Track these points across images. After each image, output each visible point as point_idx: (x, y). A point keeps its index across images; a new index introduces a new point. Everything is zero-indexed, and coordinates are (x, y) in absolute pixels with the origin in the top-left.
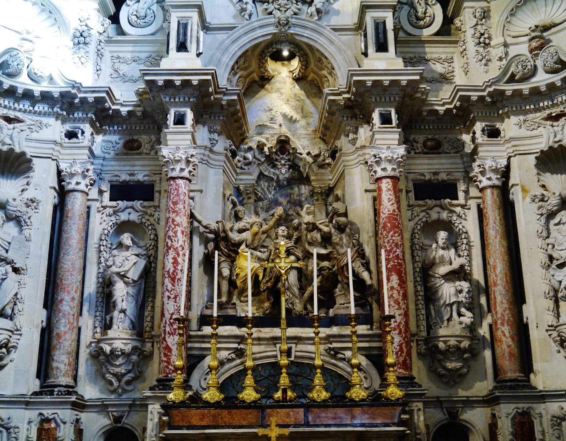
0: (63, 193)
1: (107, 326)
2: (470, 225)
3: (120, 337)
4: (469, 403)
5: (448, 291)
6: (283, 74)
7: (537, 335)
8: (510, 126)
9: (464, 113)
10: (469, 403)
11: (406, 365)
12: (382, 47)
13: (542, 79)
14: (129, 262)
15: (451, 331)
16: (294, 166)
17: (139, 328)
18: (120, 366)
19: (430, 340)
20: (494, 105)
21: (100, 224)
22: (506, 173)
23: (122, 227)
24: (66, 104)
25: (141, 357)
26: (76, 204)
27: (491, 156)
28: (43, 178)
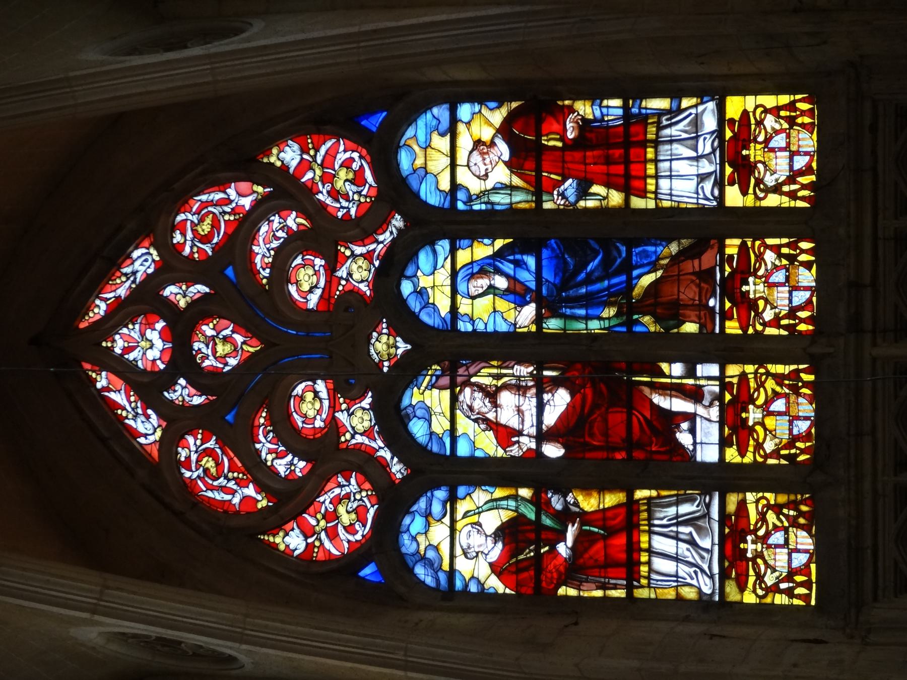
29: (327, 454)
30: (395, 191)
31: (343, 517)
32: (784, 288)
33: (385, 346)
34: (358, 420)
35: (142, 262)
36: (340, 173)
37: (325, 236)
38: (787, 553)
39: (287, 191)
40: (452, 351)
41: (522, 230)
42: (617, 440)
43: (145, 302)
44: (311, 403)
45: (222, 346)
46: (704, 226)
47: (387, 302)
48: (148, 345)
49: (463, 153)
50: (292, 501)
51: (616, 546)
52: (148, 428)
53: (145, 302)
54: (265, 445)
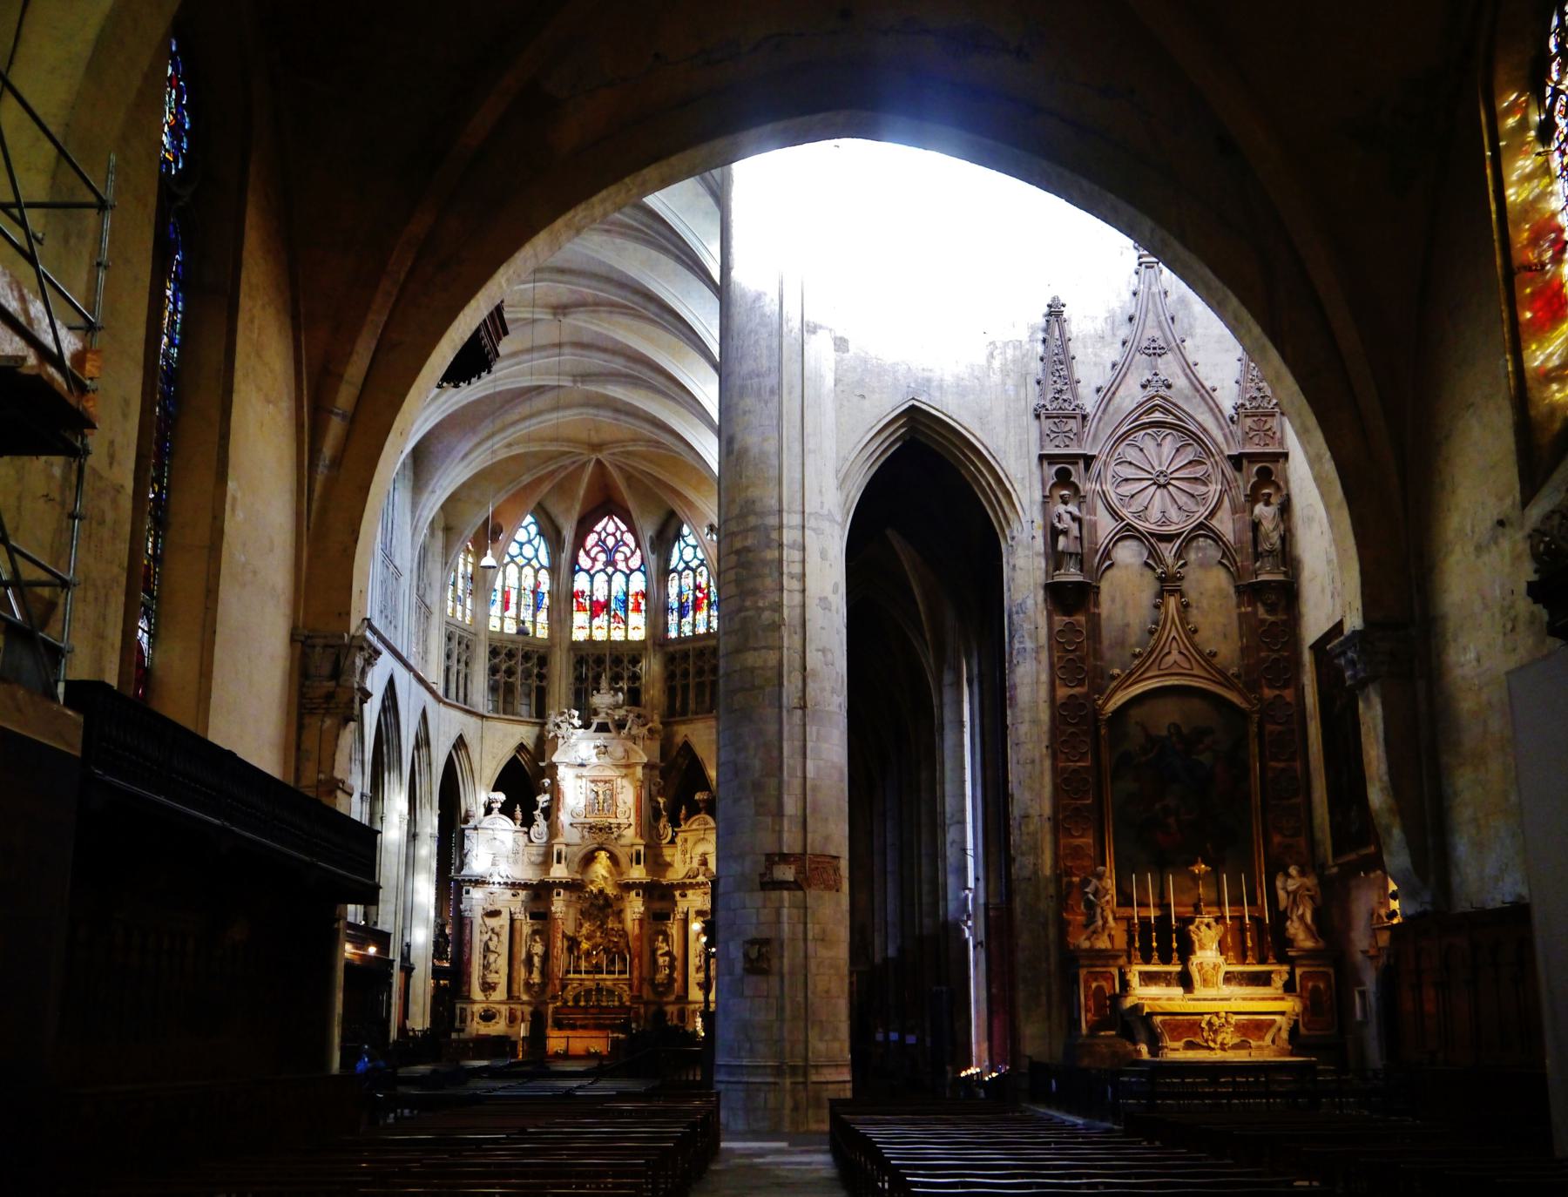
0: (512, 920)
1: (531, 972)
2: (674, 930)
3: (536, 978)
4: (668, 1003)
5: (661, 960)
6: (603, 855)
7: (690, 980)
8: (690, 893)
9: (672, 887)
10: (668, 1003)
11: (640, 990)
12: (638, 863)
13: (701, 878)
14: (538, 948)
15: (661, 976)
16: (606, 897)
17: (543, 973)
18: (536, 989)
19: (653, 980)
20: (684, 887)
21: (526, 930)
22: (687, 914)
23: (535, 932)
24: (514, 886)
25: (544, 985)
26: (517, 924)
27: (682, 905)
28: (505, 917)
29: (594, 560)
30: (632, 571)
31: (584, 561)
32: (618, 635)
33: (610, 570)
34: (599, 565)
35: (623, 527)
36: (635, 562)
37: (626, 559)
38: (579, 635)
39: (633, 553)
40: (609, 582)
41: (626, 594)
42: (597, 608)
43: (618, 528)
44: (602, 557)
45: (611, 542)
46: (626, 623)
47: (616, 570)
48: (611, 528)
49: (638, 583)
50: (587, 553)
51: (581, 608)
52: (598, 528)
53: (618, 528)
54: (597, 549)
